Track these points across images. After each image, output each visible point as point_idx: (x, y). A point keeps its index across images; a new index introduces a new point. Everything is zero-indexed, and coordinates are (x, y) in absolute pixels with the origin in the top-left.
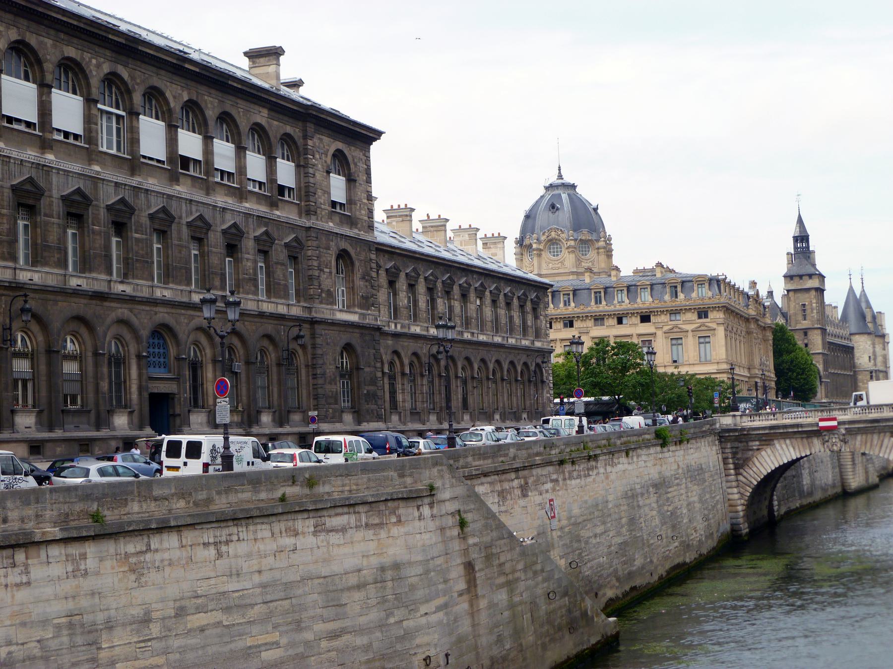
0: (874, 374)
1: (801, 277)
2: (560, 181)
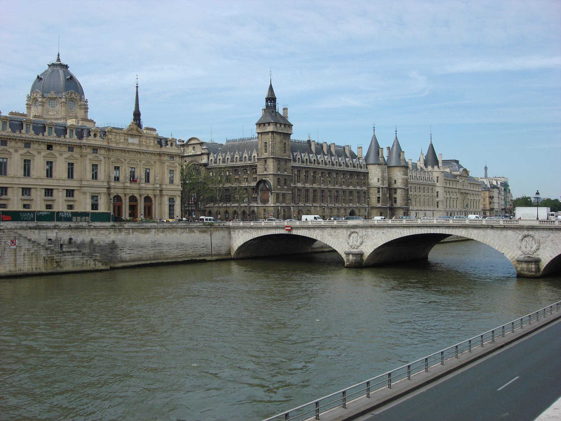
0: (381, 190)
1: (264, 124)
2: (59, 63)
